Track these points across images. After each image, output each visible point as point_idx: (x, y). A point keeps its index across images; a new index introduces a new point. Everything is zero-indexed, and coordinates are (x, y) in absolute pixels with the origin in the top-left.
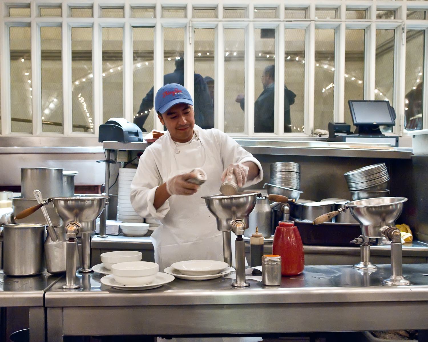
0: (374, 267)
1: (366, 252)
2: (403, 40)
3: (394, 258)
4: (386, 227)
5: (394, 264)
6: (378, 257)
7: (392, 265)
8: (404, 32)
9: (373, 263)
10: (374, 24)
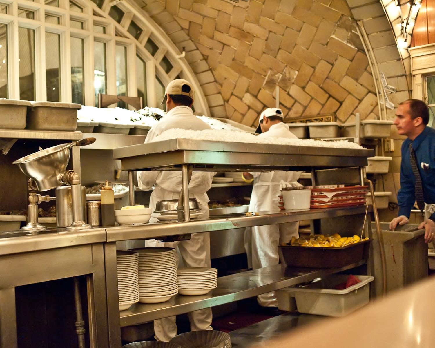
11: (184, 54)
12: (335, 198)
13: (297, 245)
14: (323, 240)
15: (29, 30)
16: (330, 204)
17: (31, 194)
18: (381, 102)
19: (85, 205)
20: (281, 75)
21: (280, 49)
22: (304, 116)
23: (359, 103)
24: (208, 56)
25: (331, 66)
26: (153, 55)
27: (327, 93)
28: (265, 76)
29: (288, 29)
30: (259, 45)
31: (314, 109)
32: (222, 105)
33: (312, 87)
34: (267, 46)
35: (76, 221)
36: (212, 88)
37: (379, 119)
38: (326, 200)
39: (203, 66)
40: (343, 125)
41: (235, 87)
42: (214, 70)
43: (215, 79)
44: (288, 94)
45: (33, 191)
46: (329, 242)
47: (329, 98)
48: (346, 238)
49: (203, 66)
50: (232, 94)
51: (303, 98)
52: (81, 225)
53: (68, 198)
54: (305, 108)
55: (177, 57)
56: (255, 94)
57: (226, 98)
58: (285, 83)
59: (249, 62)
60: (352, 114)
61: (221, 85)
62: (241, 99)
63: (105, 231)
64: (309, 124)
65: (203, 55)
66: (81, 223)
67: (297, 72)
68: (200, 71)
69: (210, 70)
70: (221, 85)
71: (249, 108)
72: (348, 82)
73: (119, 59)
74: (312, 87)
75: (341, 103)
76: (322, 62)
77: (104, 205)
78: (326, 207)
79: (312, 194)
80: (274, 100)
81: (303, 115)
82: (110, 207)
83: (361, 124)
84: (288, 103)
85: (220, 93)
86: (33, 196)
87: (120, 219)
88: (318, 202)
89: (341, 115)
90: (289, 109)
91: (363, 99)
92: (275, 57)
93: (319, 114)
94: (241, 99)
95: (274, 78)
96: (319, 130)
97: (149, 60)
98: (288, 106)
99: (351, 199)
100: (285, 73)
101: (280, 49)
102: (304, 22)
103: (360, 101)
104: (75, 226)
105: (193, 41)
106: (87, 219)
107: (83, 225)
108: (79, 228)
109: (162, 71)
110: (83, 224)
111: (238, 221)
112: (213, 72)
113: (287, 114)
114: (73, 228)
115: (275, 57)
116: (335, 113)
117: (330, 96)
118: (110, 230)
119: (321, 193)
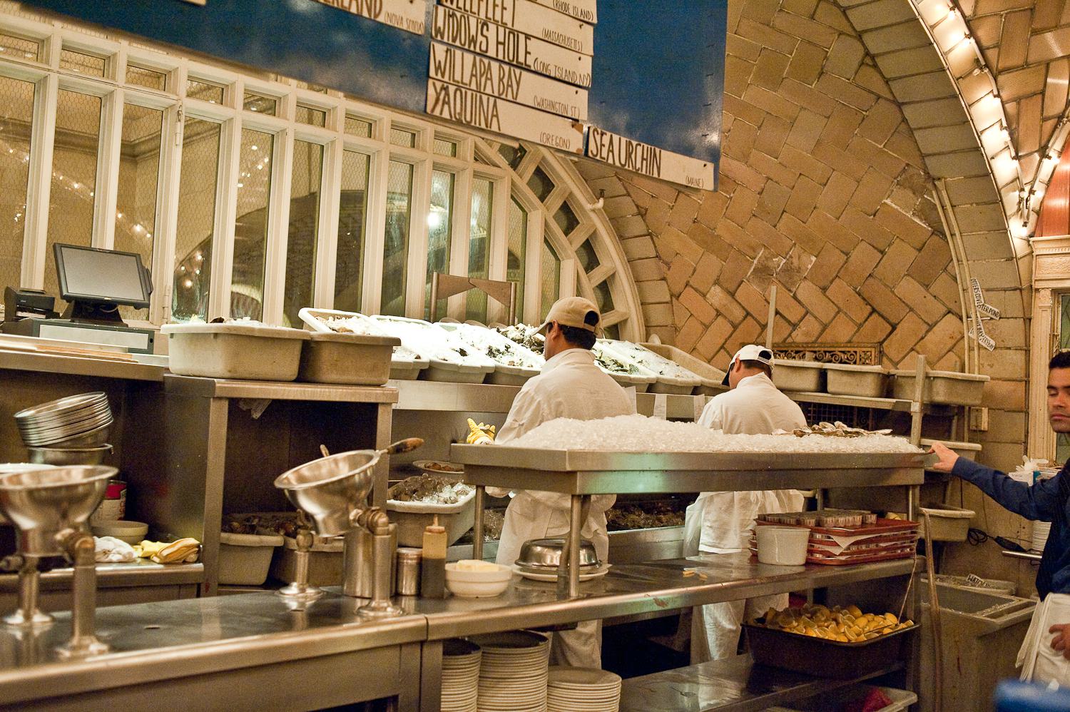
0: (47, 619)
1: (31, 586)
2: (178, 135)
3: (78, 597)
4: (67, 531)
5: (77, 612)
6: (55, 593)
7: (74, 615)
8: (179, 121)
9: (46, 610)
10: (124, 93)
11: (601, 202)
12: (854, 548)
13: (777, 628)
14: (825, 621)
15: (310, 144)
16: (843, 558)
17: (302, 531)
18: (970, 335)
19: (395, 555)
20: (785, 261)
21: (784, 211)
22: (821, 343)
23: (928, 332)
24: (646, 210)
25: (881, 256)
26: (542, 198)
27: (868, 304)
28: (755, 258)
29: (802, 177)
30: (745, 200)
31: (842, 332)
32: (667, 303)
33: (840, 290)
34: (760, 204)
35: (377, 600)
36: (650, 269)
37: (963, 370)
38: (836, 551)
39: (637, 226)
40: (893, 371)
41: (695, 271)
42: (657, 236)
43: (657, 252)
44: (795, 297)
45: (305, 528)
46: (838, 624)
47: (871, 314)
48: (871, 616)
49: (637, 226)
50: (687, 284)
51: (822, 309)
52: (386, 608)
53: (364, 546)
54: (825, 327)
55: (588, 207)
56: (732, 289)
57: (676, 290)
58: (790, 276)
59: (724, 229)
60: (912, 350)
61: (668, 265)
62: (704, 296)
63: (425, 622)
64: (827, 366)
65: (637, 206)
66: (385, 605)
67: (814, 259)
68: (627, 235)
69: (650, 234)
70: (668, 265)
71: (719, 314)
72: (909, 289)
73: (477, 204)
74: (840, 290)
75: (894, 328)
76: (863, 245)
77: (427, 560)
78: (835, 563)
79: (811, 535)
80: (766, 303)
81: (819, 340)
82: (439, 564)
83: (927, 377)
84: (794, 313)
85: (664, 279)
86: (305, 536)
87: (455, 587)
88: (821, 552)
89: (891, 348)
90: (794, 326)
91: (936, 323)
92: (775, 226)
93: (850, 342)
94: (704, 296)
95: (770, 264)
96: (845, 379)
97: (536, 209)
98: (794, 319)
99: (885, 549)
100: (791, 257)
101: (784, 211)
102: (834, 170)
103: (931, 327)
104: (373, 609)
105: (620, 179)
106: (396, 596)
107: (389, 609)
108: (381, 614)
109: (557, 230)
110: (388, 606)
111: (670, 596)
112: (655, 238)
113: (790, 335)
114: (372, 614)
115: (775, 226)
116: (881, 343)
117: (874, 311)
118: (436, 618)
119: (829, 538)
